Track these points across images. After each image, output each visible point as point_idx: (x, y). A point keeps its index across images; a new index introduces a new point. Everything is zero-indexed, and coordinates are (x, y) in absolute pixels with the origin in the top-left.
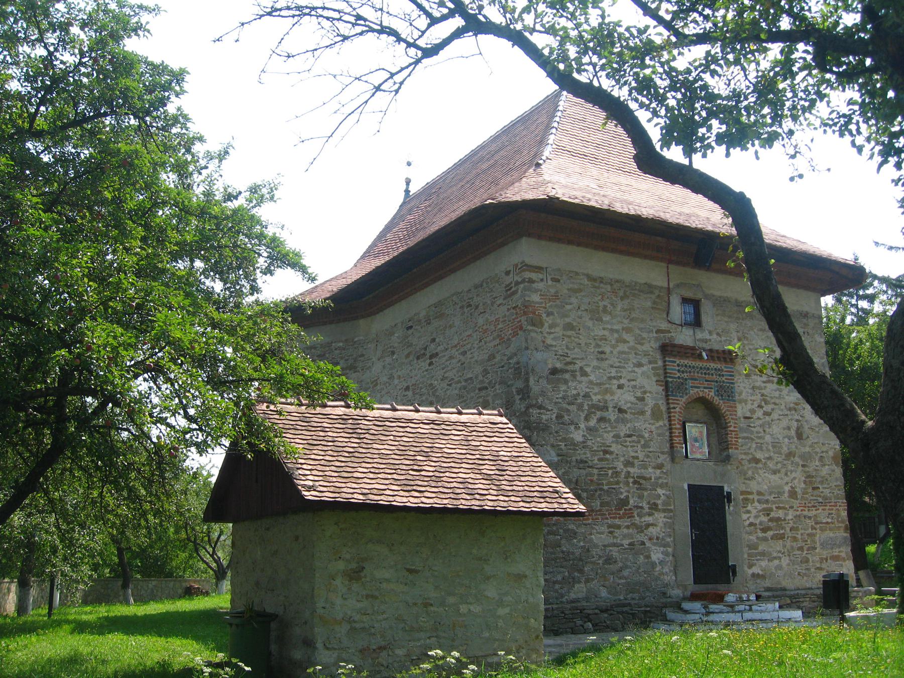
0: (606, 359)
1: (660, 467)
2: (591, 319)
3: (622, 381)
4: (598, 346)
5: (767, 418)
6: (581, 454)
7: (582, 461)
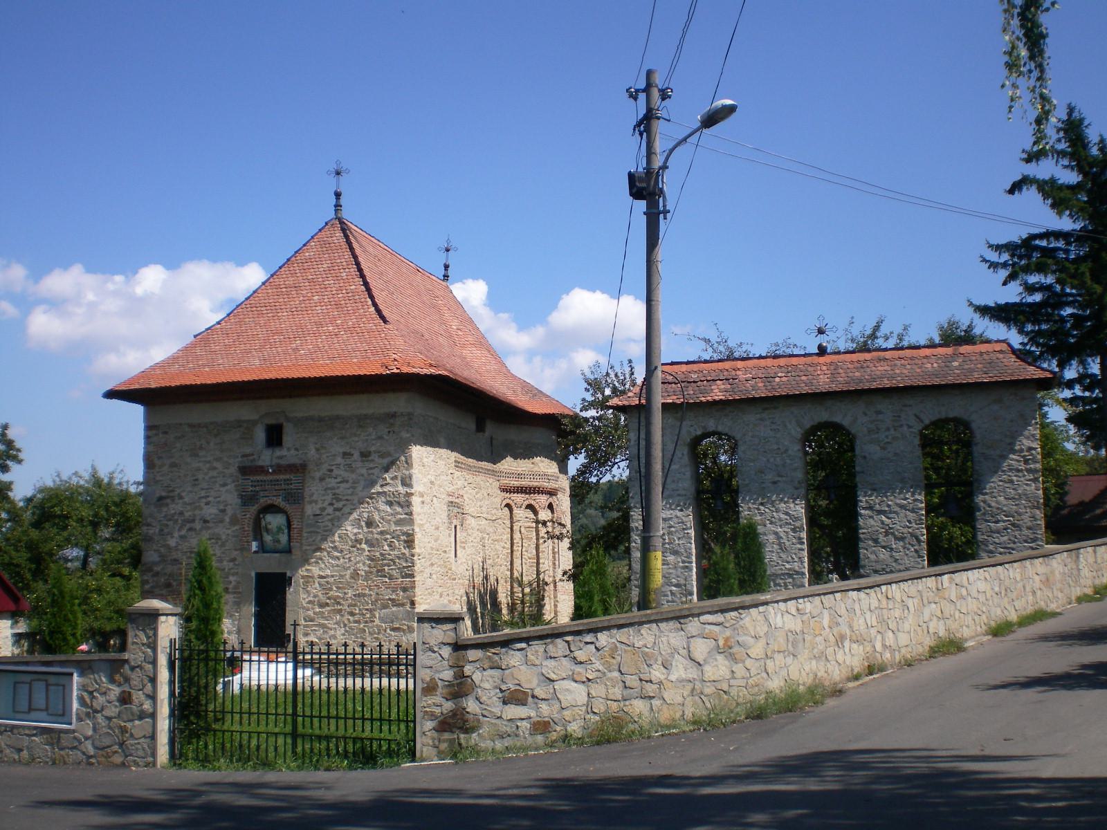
0: (198, 484)
1: (233, 560)
2: (191, 456)
3: (210, 499)
4: (194, 476)
5: (337, 513)
6: (175, 555)
7: (176, 560)
